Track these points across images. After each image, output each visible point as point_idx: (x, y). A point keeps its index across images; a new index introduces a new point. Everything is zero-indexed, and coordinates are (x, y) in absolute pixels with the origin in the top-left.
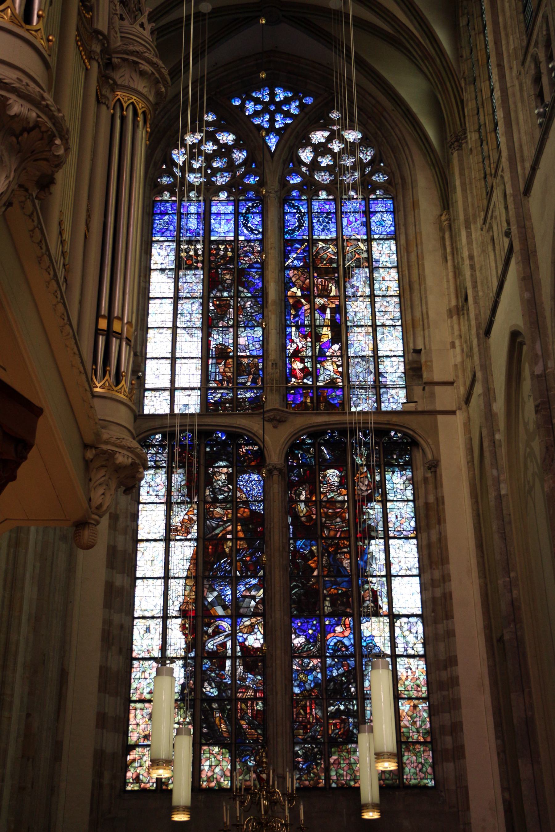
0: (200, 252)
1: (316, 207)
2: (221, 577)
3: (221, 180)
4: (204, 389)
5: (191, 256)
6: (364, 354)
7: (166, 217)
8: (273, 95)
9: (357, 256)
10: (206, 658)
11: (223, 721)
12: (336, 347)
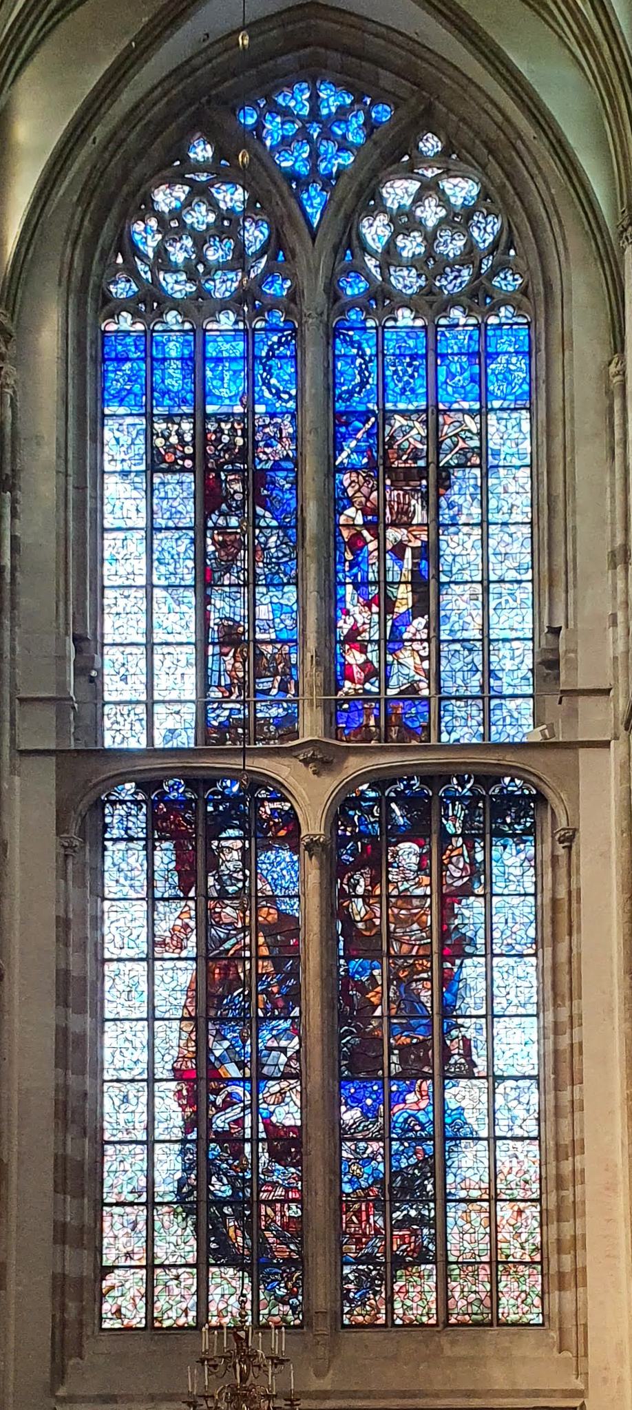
0: (188, 438)
1: (392, 344)
2: (234, 1018)
3: (223, 286)
4: (203, 706)
5: (172, 446)
6: (466, 635)
7: (127, 366)
9: (461, 444)
10: (213, 1141)
11: (239, 1232)
12: (420, 622)
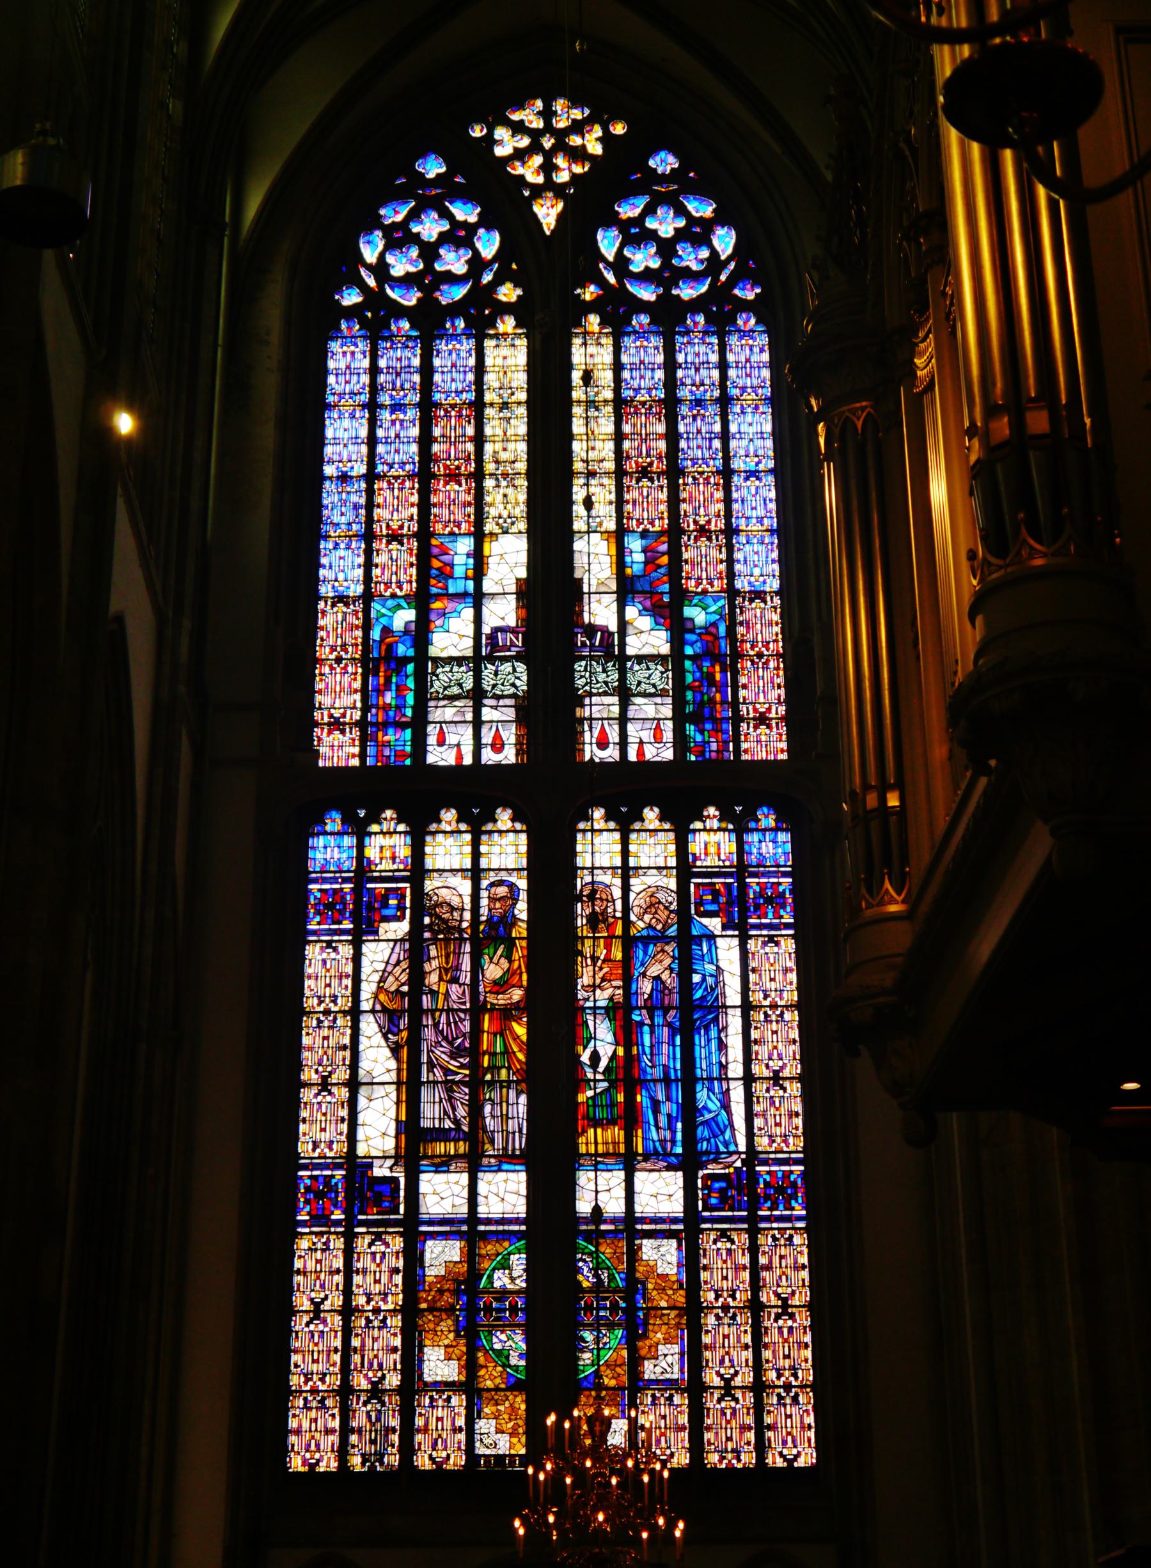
8: (547, 114)
